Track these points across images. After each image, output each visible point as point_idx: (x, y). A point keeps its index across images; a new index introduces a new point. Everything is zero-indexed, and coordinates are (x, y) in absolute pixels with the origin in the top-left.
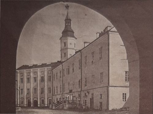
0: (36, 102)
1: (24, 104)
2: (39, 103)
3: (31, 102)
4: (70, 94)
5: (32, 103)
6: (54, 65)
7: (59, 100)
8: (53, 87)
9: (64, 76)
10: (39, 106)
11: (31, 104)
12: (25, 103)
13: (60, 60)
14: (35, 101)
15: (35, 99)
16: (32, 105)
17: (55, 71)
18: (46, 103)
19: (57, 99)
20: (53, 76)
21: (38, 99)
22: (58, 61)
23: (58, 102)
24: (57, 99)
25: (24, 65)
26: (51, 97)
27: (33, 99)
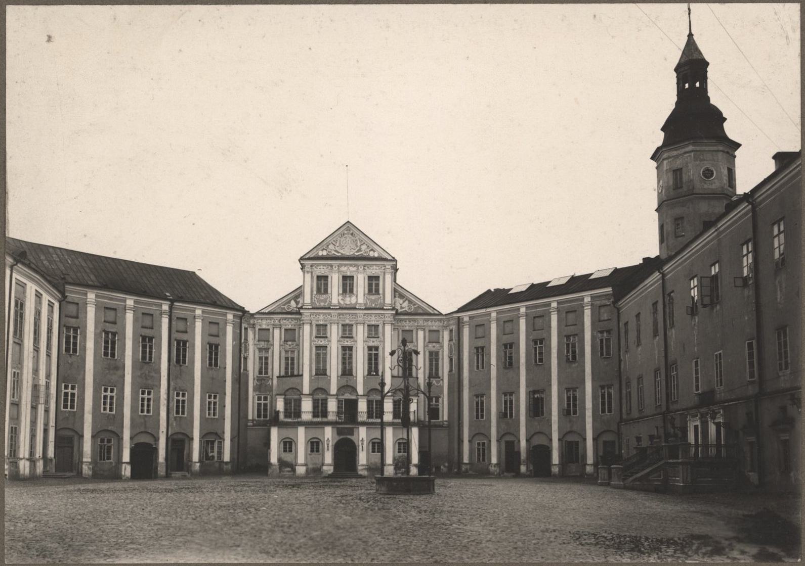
0: (540, 454)
1: (490, 463)
2: (555, 458)
3: (519, 453)
4: (703, 410)
5: (523, 455)
6: (624, 280)
7: (645, 443)
8: (624, 383)
9: (672, 325)
10: (555, 470)
11: (519, 464)
12: (494, 460)
13: (653, 251)
14: (536, 447)
15: (537, 441)
16: (523, 469)
17: (631, 303)
18: (590, 460)
19: (639, 439)
20: (623, 331)
21: (551, 440)
22: (647, 260)
23: (642, 451)
24: (639, 439)
25: (489, 290)
26: (614, 427)
27: (527, 441)
